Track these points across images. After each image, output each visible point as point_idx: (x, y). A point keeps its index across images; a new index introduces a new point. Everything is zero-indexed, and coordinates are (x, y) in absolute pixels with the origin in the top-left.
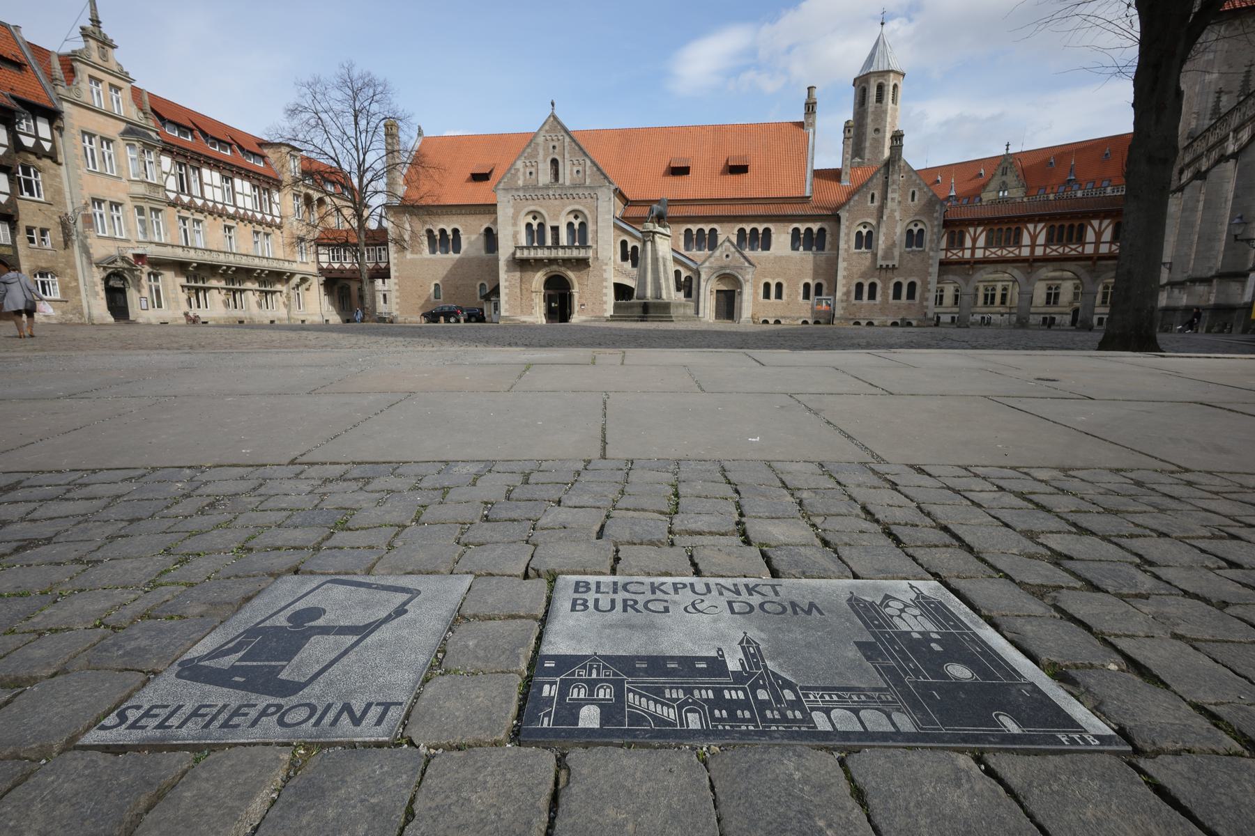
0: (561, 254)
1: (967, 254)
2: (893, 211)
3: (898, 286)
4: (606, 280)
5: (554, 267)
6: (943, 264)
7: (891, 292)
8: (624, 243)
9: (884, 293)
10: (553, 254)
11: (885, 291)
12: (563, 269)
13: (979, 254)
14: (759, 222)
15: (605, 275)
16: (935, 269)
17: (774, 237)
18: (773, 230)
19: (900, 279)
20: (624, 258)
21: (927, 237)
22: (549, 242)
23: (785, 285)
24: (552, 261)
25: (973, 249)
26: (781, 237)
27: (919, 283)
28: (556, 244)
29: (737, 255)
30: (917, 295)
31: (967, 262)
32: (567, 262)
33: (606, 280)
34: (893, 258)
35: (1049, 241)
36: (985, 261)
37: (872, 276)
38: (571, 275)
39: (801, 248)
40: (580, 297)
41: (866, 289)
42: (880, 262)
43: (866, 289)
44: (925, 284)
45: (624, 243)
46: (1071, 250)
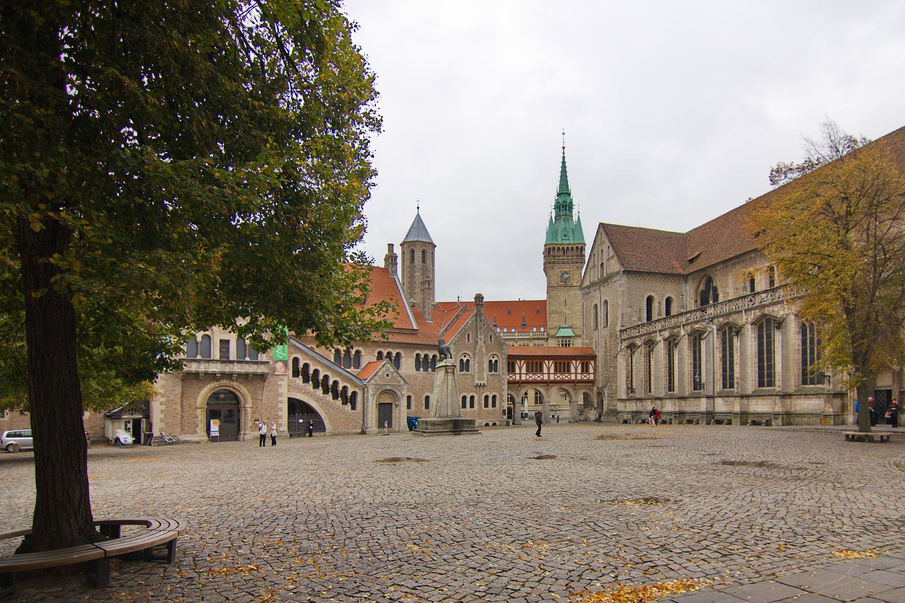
0: (237, 368)
1: (518, 378)
2: (481, 347)
3: (487, 397)
4: (281, 395)
5: (225, 382)
6: (509, 383)
7: (483, 402)
8: (296, 360)
9: (480, 403)
10: (228, 368)
11: (479, 401)
12: (235, 384)
13: (524, 378)
14: (393, 348)
15: (280, 390)
16: (505, 387)
17: (403, 360)
18: (403, 355)
19: (488, 394)
20: (296, 374)
21: (500, 365)
22: (216, 354)
23: (413, 398)
24: (229, 376)
25: (520, 374)
26: (408, 363)
27: (498, 396)
28: (225, 358)
29: (395, 374)
30: (497, 404)
31: (518, 382)
32: (245, 377)
33: (281, 395)
34: (483, 379)
35: (528, 371)
36: (527, 382)
37: (472, 391)
38: (243, 390)
39: (422, 369)
40: (254, 412)
41: (468, 400)
42: (476, 382)
43: (468, 400)
44: (502, 396)
45: (296, 360)
46: (565, 377)
